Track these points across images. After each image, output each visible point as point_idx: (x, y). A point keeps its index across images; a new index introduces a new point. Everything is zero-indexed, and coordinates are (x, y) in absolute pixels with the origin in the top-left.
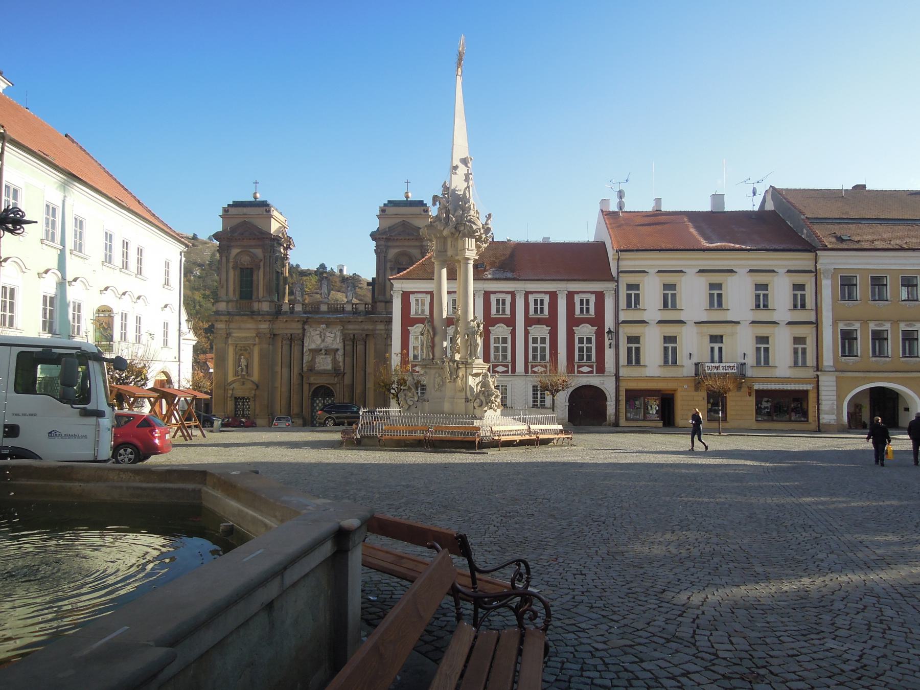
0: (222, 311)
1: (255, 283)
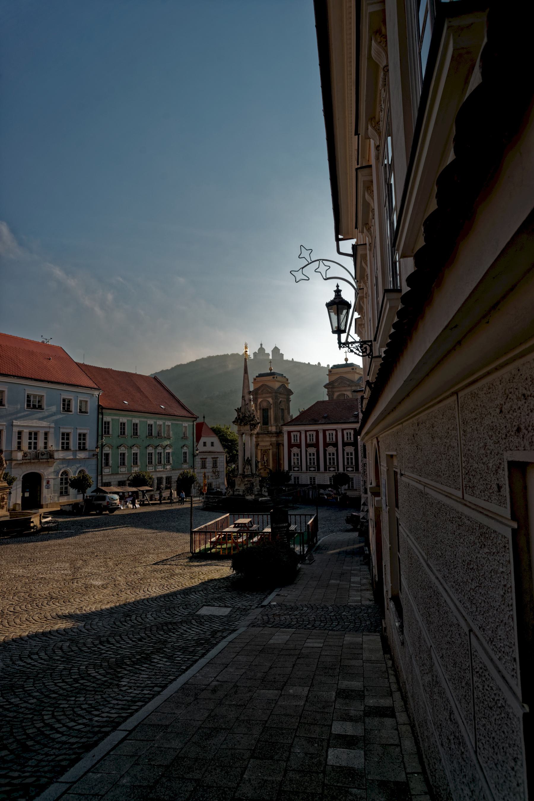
1: (269, 416)
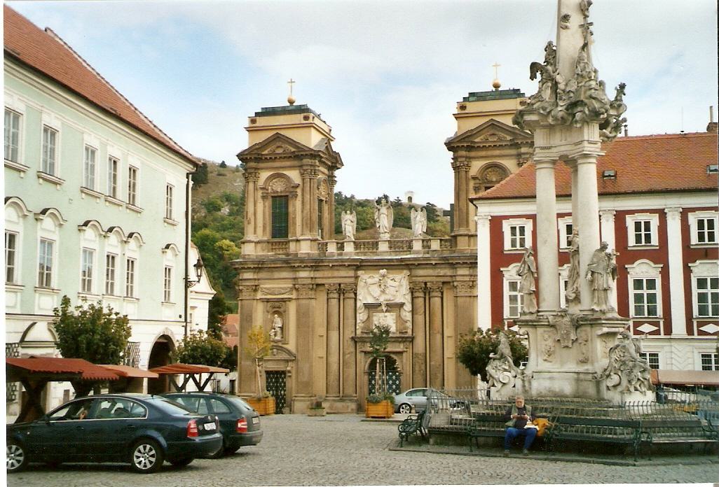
0: (249, 255)
1: (291, 216)
